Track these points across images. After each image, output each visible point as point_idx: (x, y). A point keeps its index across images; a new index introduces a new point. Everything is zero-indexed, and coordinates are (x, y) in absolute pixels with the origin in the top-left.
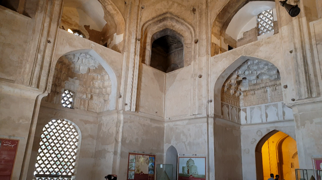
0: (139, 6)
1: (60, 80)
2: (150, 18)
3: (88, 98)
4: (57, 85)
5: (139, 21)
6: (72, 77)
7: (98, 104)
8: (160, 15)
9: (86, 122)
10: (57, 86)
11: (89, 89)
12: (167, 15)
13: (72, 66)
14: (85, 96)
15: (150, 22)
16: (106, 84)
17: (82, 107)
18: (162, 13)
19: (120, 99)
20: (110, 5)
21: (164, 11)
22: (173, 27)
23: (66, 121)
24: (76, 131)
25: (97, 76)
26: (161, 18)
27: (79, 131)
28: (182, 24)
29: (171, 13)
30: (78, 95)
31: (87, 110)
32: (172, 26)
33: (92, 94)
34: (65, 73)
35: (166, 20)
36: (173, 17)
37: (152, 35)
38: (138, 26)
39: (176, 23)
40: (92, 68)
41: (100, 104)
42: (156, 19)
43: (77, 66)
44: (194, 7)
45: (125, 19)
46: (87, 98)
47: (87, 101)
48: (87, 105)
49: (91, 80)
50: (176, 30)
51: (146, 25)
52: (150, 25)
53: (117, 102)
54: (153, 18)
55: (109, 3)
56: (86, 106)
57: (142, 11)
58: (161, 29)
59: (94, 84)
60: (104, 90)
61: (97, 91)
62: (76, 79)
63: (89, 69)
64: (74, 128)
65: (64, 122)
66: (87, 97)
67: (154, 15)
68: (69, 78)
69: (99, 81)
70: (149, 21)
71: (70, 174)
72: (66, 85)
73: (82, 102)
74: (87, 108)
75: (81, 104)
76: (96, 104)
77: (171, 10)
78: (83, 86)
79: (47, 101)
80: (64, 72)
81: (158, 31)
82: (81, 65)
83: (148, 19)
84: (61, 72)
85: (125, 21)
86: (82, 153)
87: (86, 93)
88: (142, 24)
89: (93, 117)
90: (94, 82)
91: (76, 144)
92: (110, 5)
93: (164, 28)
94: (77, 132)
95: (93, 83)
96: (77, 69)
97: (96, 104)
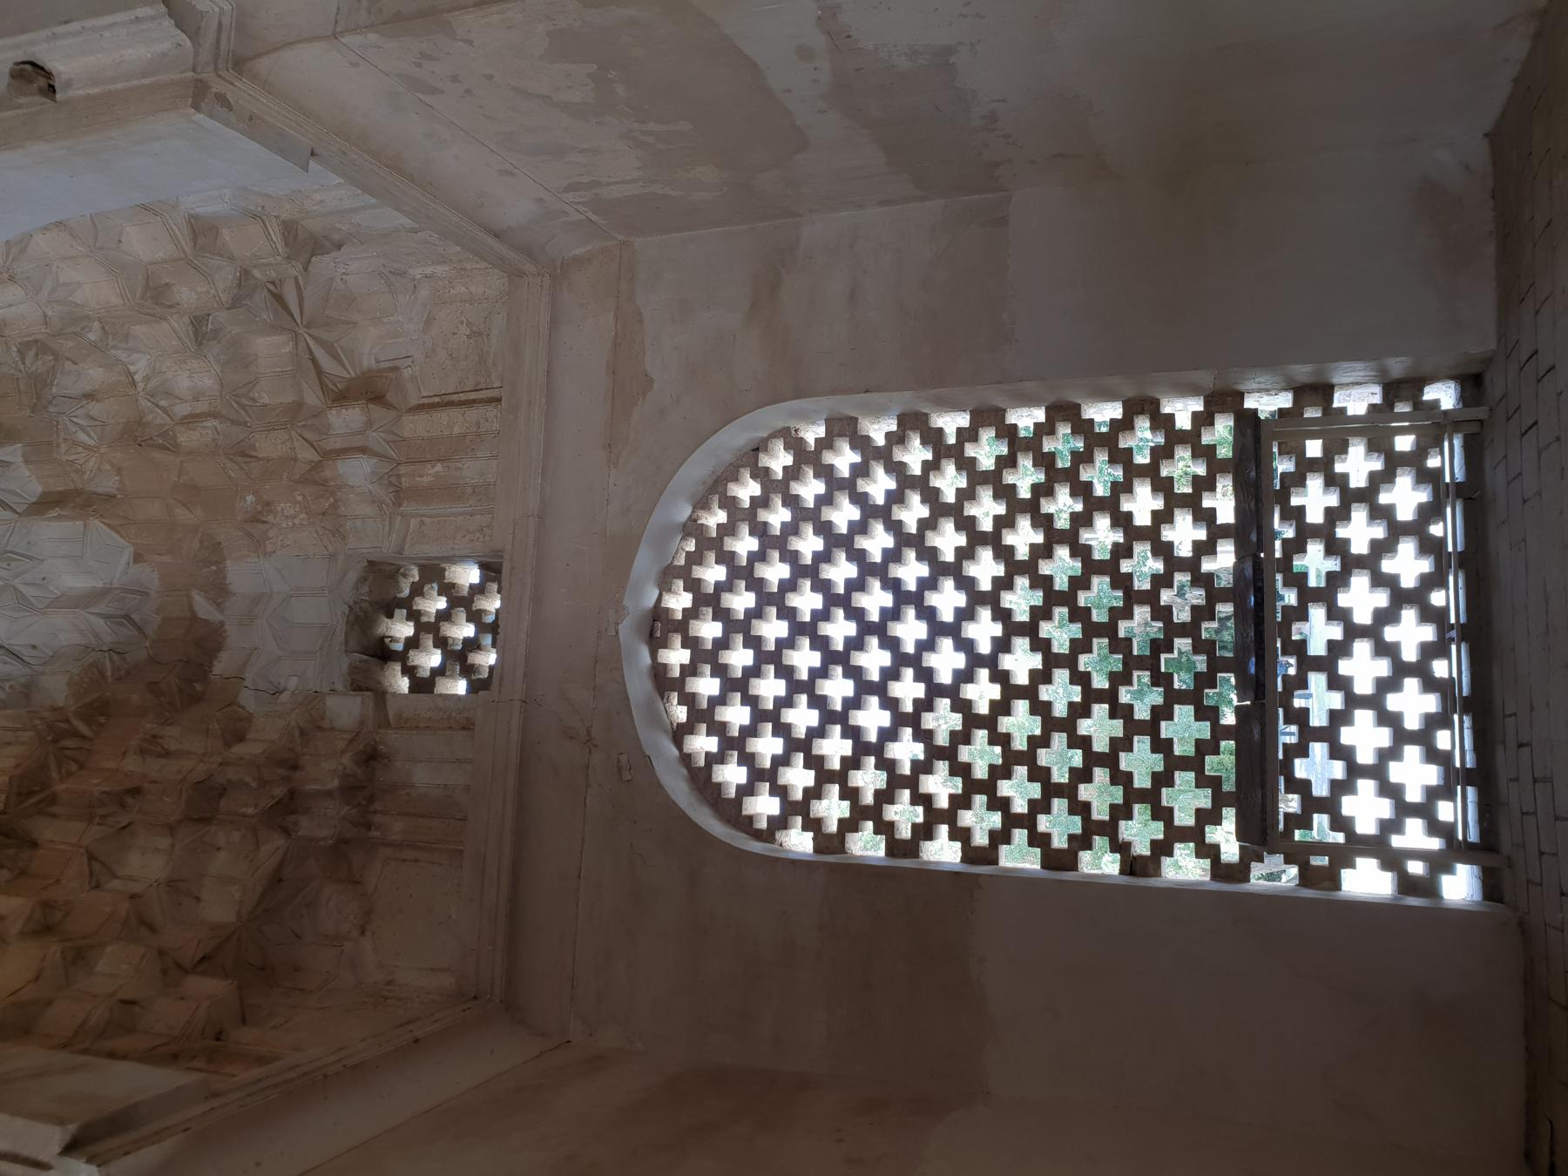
1: (232, 774)
3: (370, 423)
4: (279, 791)
6: (208, 641)
7: (424, 292)
9: (626, 383)
10: (292, 794)
11: (270, 446)
13: (57, 689)
14: (357, 472)
16: (93, 289)
17: (470, 470)
19: (59, 66)
23: (665, 586)
24: (750, 459)
25: (90, 396)
27: (735, 437)
30: (371, 535)
31: (491, 411)
33: (312, 398)
34: (151, 747)
40: (25, 472)
41: (417, 272)
43: (64, 631)
46: (375, 438)
47: (416, 427)
48: (443, 416)
49: (158, 455)
53: (110, 107)
56: (452, 422)
59: (202, 407)
60: (187, 294)
61: (270, 348)
62: (219, 591)
63: (47, 503)
64: (716, 489)
65: (679, 601)
66: (357, 441)
68: (222, 665)
69: (140, 366)
71: (1222, 431)
72: (293, 683)
73: (426, 480)
74: (473, 414)
75: (451, 491)
76: (429, 321)
78: (256, 519)
79: (461, 852)
80: (132, 764)
82: (29, 592)
84: (136, 791)
86: (954, 349)
87: (316, 466)
89: (554, 323)
90: (182, 410)
91: (878, 431)
94: (760, 447)
95: (191, 420)
96: (96, 626)
97: (429, 321)
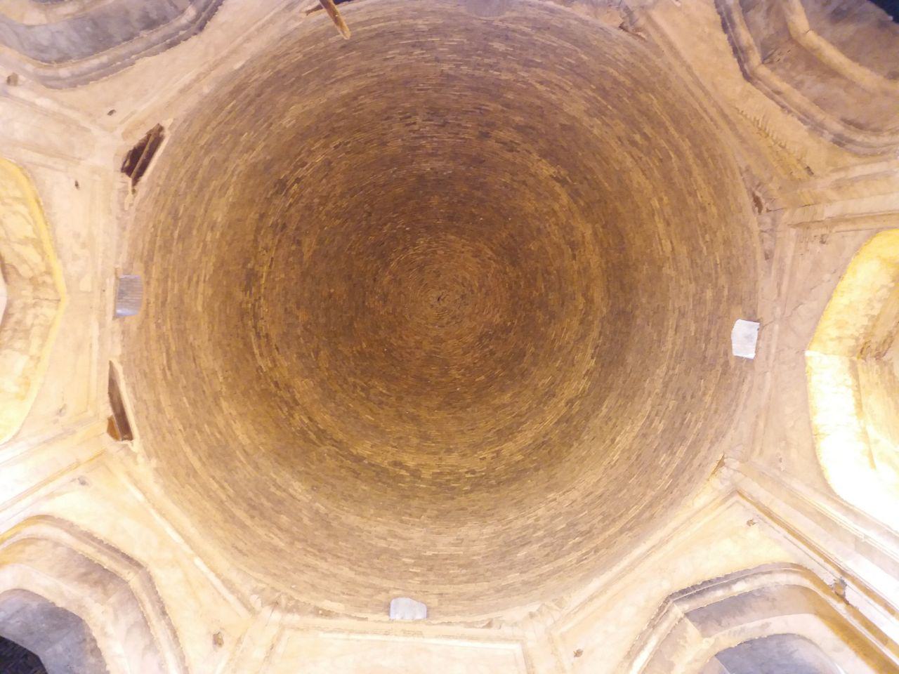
0: (78, 464)
2: (85, 523)
5: (43, 492)
8: (114, 551)
12: (132, 574)
15: (65, 537)
18: (128, 552)
20: (31, 357)
21: (138, 553)
22: (105, 634)
26: (107, 562)
28: (152, 645)
29: (149, 580)
32: (103, 629)
35: (105, 592)
36: (144, 597)
37: (15, 586)
38: (29, 500)
39: (129, 631)
42: (89, 550)
44: (222, 632)
45: (18, 433)
50: (106, 655)
51: (44, 529)
52: (57, 544)
54: (89, 537)
55: (34, 350)
57: (73, 483)
58: (61, 604)
67: (101, 531)
70: (70, 527)
77: (157, 572)
81: (46, 595)
83: (72, 518)
85: (14, 437)
88: (45, 508)
92: (26, 358)
93: (73, 609)
